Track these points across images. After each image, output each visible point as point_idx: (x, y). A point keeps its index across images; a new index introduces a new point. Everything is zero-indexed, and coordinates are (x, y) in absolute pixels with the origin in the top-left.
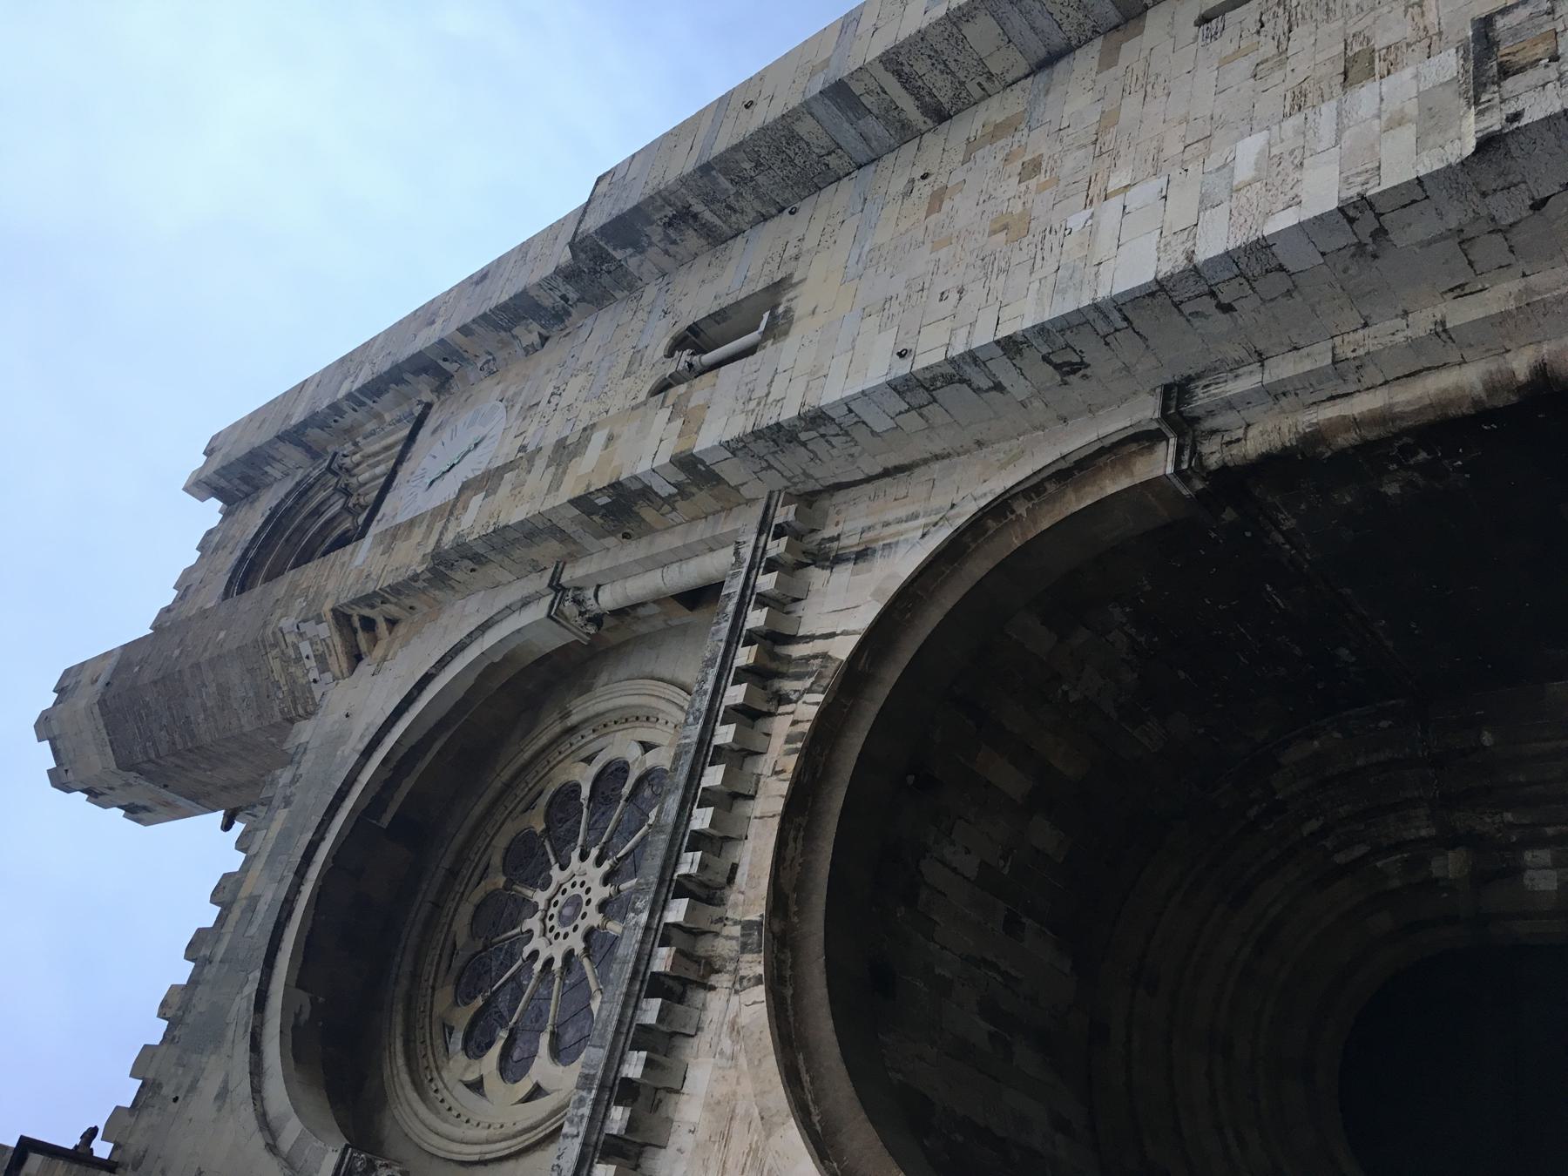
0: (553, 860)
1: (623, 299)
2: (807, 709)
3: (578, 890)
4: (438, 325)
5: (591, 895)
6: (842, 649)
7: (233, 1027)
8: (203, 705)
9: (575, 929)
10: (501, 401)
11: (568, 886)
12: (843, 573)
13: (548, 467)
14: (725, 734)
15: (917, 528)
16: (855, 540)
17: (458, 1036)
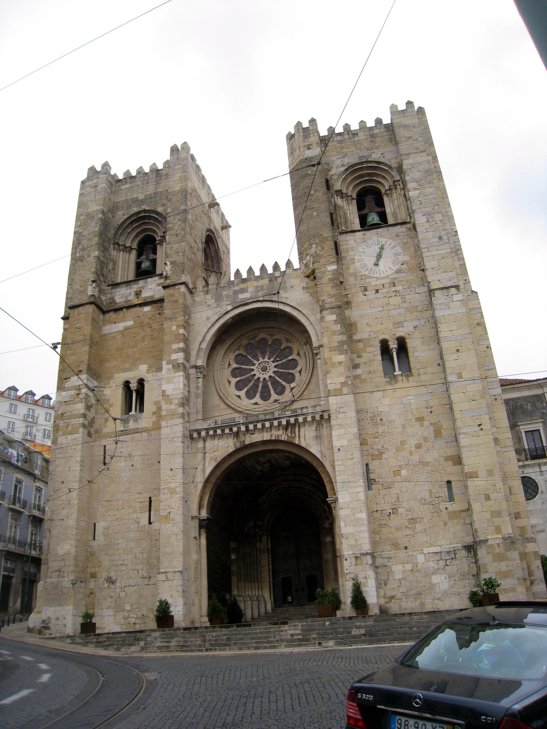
2: (284, 438)
3: (268, 368)
4: (427, 225)
5: (267, 373)
10: (402, 264)
11: (269, 365)
13: (338, 342)
15: (321, 449)
16: (322, 434)
17: (237, 353)
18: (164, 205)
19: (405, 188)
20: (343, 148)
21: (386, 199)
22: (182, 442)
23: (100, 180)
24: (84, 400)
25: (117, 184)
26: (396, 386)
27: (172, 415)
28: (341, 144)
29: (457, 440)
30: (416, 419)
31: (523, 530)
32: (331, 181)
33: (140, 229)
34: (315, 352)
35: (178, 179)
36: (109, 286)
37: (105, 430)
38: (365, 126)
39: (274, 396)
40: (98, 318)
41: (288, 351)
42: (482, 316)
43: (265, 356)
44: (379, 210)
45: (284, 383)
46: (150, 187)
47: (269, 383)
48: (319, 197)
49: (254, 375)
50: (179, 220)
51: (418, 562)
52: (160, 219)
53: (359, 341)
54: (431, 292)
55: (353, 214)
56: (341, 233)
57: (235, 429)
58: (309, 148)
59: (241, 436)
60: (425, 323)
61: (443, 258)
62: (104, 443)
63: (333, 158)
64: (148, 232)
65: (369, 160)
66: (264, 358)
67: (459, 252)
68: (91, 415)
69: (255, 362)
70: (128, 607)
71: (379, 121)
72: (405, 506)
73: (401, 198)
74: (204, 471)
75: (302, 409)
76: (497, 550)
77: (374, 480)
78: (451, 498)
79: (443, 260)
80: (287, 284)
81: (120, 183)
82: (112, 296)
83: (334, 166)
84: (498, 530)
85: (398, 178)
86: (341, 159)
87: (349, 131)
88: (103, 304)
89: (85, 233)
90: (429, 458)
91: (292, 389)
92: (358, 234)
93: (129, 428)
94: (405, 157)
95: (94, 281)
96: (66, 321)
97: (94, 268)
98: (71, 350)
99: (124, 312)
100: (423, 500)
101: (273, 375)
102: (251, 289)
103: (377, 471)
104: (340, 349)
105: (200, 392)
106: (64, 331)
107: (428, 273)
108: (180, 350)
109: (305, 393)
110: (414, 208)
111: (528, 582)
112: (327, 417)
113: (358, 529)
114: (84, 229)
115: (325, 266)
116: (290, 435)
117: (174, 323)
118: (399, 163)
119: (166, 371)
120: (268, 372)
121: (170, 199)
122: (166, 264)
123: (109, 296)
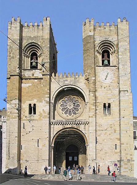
12: (84, 127)
31: (132, 158)
52: (39, 47)
53: (98, 102)
54: (120, 91)
56: (97, 66)
57: (63, 123)
62: (24, 122)
65: (108, 40)
70: (32, 168)
74: (53, 133)
75: (81, 120)
78: (116, 149)
82: (24, 74)
84: (126, 158)
102: (69, 80)
118: (117, 43)
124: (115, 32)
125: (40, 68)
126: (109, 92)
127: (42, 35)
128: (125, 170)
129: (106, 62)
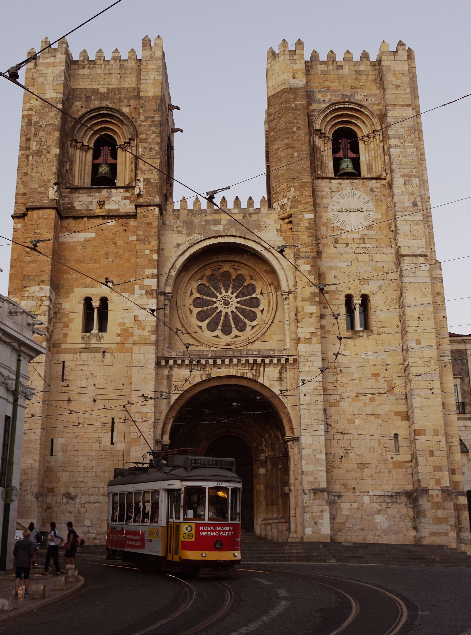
0: (238, 291)
1: (395, 263)
2: (249, 375)
4: (403, 188)
5: (230, 308)
6: (260, 380)
7: (191, 238)
8: (278, 149)
9: (223, 307)
10: (373, 222)
11: (232, 300)
12: (277, 375)
13: (311, 293)
14: (243, 361)
16: (285, 376)
18: (130, 106)
19: (384, 139)
20: (326, 80)
21: (361, 146)
22: (155, 369)
23: (57, 60)
24: (47, 313)
25: (73, 66)
26: (358, 341)
27: (143, 342)
28: (325, 75)
29: (406, 399)
30: (372, 374)
32: (311, 117)
33: (99, 127)
34: (284, 297)
35: (152, 82)
36: (66, 189)
37: (64, 346)
38: (351, 59)
39: (235, 332)
40: (57, 223)
41: (250, 288)
42: (443, 287)
43: (228, 290)
44: (354, 156)
45: (245, 320)
46: (113, 80)
47: (231, 318)
48: (303, 137)
49: (217, 308)
50: (154, 133)
51: (364, 502)
54: (399, 257)
55: (328, 156)
57: (203, 361)
58: (294, 77)
59: (207, 369)
60: (389, 284)
61: (415, 225)
63: (317, 90)
64: (106, 131)
65: (352, 100)
66: (227, 292)
67: (429, 219)
68: (51, 329)
69: (218, 294)
71: (365, 56)
72: (356, 452)
73: (379, 150)
74: (169, 398)
76: (436, 500)
77: (330, 425)
79: (414, 227)
80: (261, 224)
81: (77, 66)
82: (70, 201)
83: (316, 99)
84: (438, 482)
85: (379, 127)
86: (323, 93)
87: (333, 61)
88: (60, 208)
89: (43, 123)
90: (380, 411)
91: (253, 327)
92: (334, 181)
93: (92, 346)
94: (391, 108)
95: (55, 184)
96: (17, 220)
97: (55, 168)
98: (31, 256)
99: (85, 223)
100: (372, 448)
101: (235, 311)
102: (224, 222)
103: (334, 417)
104: (312, 300)
105: (167, 320)
106: (14, 231)
107: (399, 237)
108: (152, 276)
109: (266, 334)
110: (394, 166)
111: (458, 529)
112: (292, 362)
113: (317, 469)
114: (41, 118)
115: (303, 213)
116: (254, 374)
117: (147, 246)
118: (381, 110)
119: (139, 295)
120: (230, 307)
121: (143, 104)
122: (139, 180)
123: (66, 200)
124: (372, 78)
125: (127, 183)
126: (364, 258)
127: (133, 86)
128: (435, 528)
129: (347, 165)
